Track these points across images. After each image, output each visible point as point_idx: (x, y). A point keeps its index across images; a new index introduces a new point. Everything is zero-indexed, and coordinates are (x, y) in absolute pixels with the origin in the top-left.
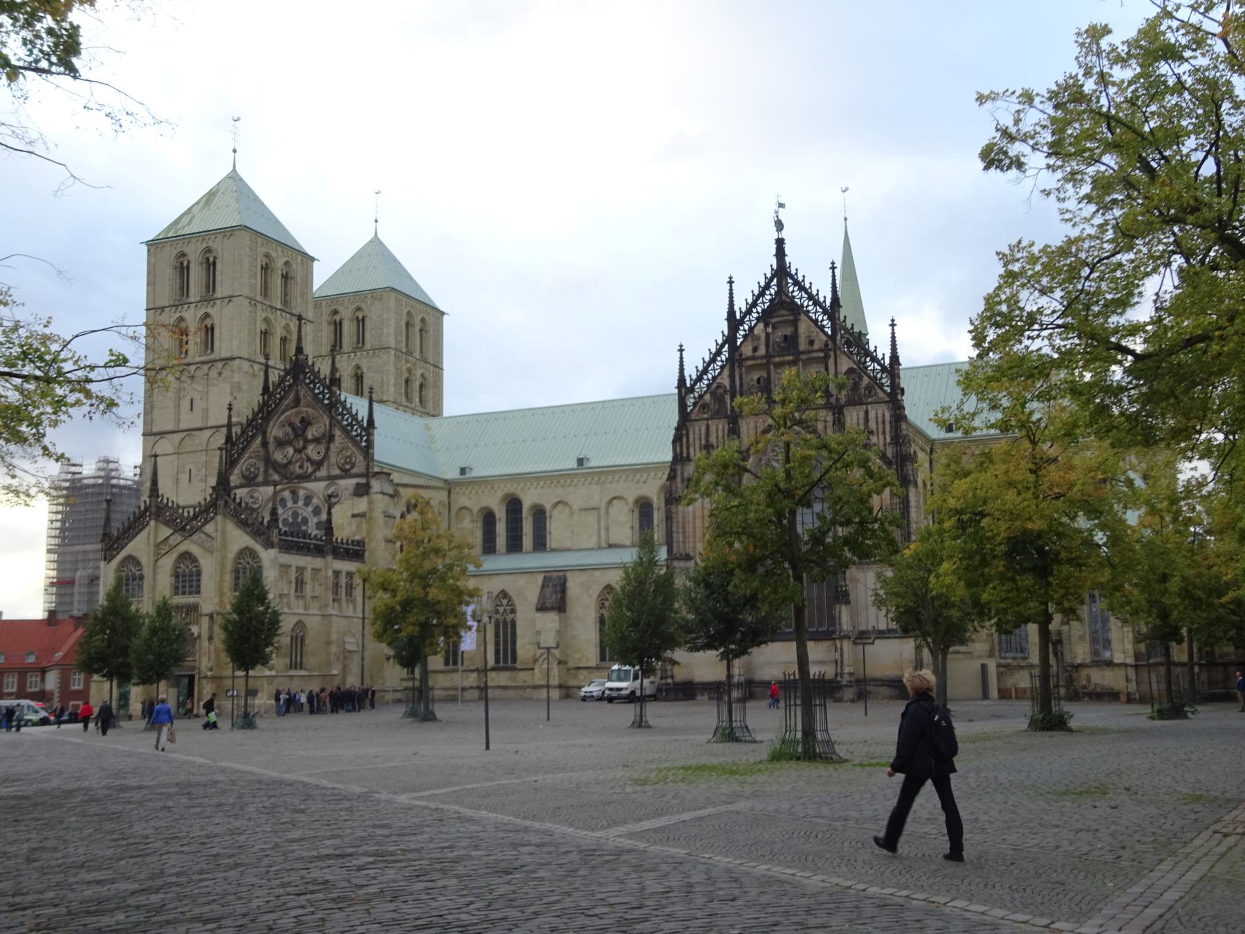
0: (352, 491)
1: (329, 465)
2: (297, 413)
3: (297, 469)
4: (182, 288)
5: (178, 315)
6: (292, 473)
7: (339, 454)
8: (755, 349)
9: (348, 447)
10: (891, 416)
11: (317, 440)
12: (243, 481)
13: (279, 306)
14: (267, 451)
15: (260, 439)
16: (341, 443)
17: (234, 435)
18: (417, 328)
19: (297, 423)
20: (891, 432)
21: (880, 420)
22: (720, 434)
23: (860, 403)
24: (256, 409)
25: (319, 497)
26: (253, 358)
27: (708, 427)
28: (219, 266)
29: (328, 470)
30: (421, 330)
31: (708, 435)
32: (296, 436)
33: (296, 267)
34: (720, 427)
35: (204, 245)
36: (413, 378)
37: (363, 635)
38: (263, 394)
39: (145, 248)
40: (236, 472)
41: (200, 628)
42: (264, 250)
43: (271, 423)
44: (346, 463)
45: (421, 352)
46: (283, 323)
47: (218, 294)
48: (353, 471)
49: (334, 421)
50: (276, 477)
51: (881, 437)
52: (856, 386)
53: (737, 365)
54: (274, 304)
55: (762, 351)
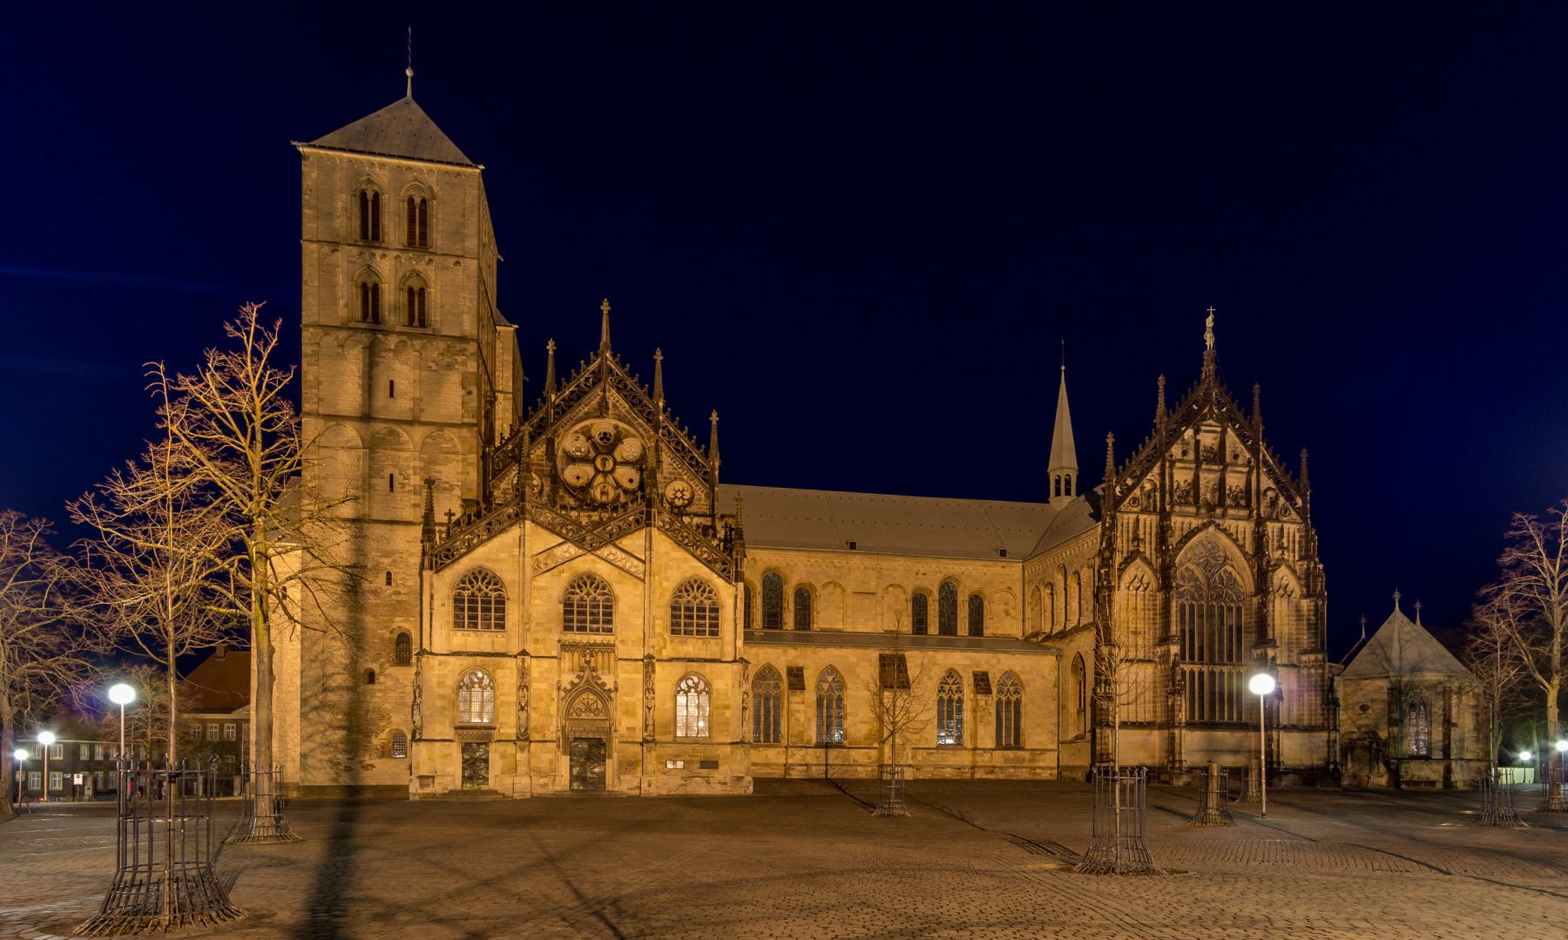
6: (594, 500)
8: (1184, 453)
10: (1300, 537)
14: (555, 467)
16: (671, 473)
19: (597, 439)
20: (1300, 551)
21: (1291, 539)
22: (1148, 530)
23: (1277, 520)
27: (1137, 520)
31: (1136, 528)
32: (598, 453)
34: (1148, 523)
49: (662, 445)
51: (1291, 554)
52: (1273, 503)
53: (1167, 464)
55: (1191, 456)
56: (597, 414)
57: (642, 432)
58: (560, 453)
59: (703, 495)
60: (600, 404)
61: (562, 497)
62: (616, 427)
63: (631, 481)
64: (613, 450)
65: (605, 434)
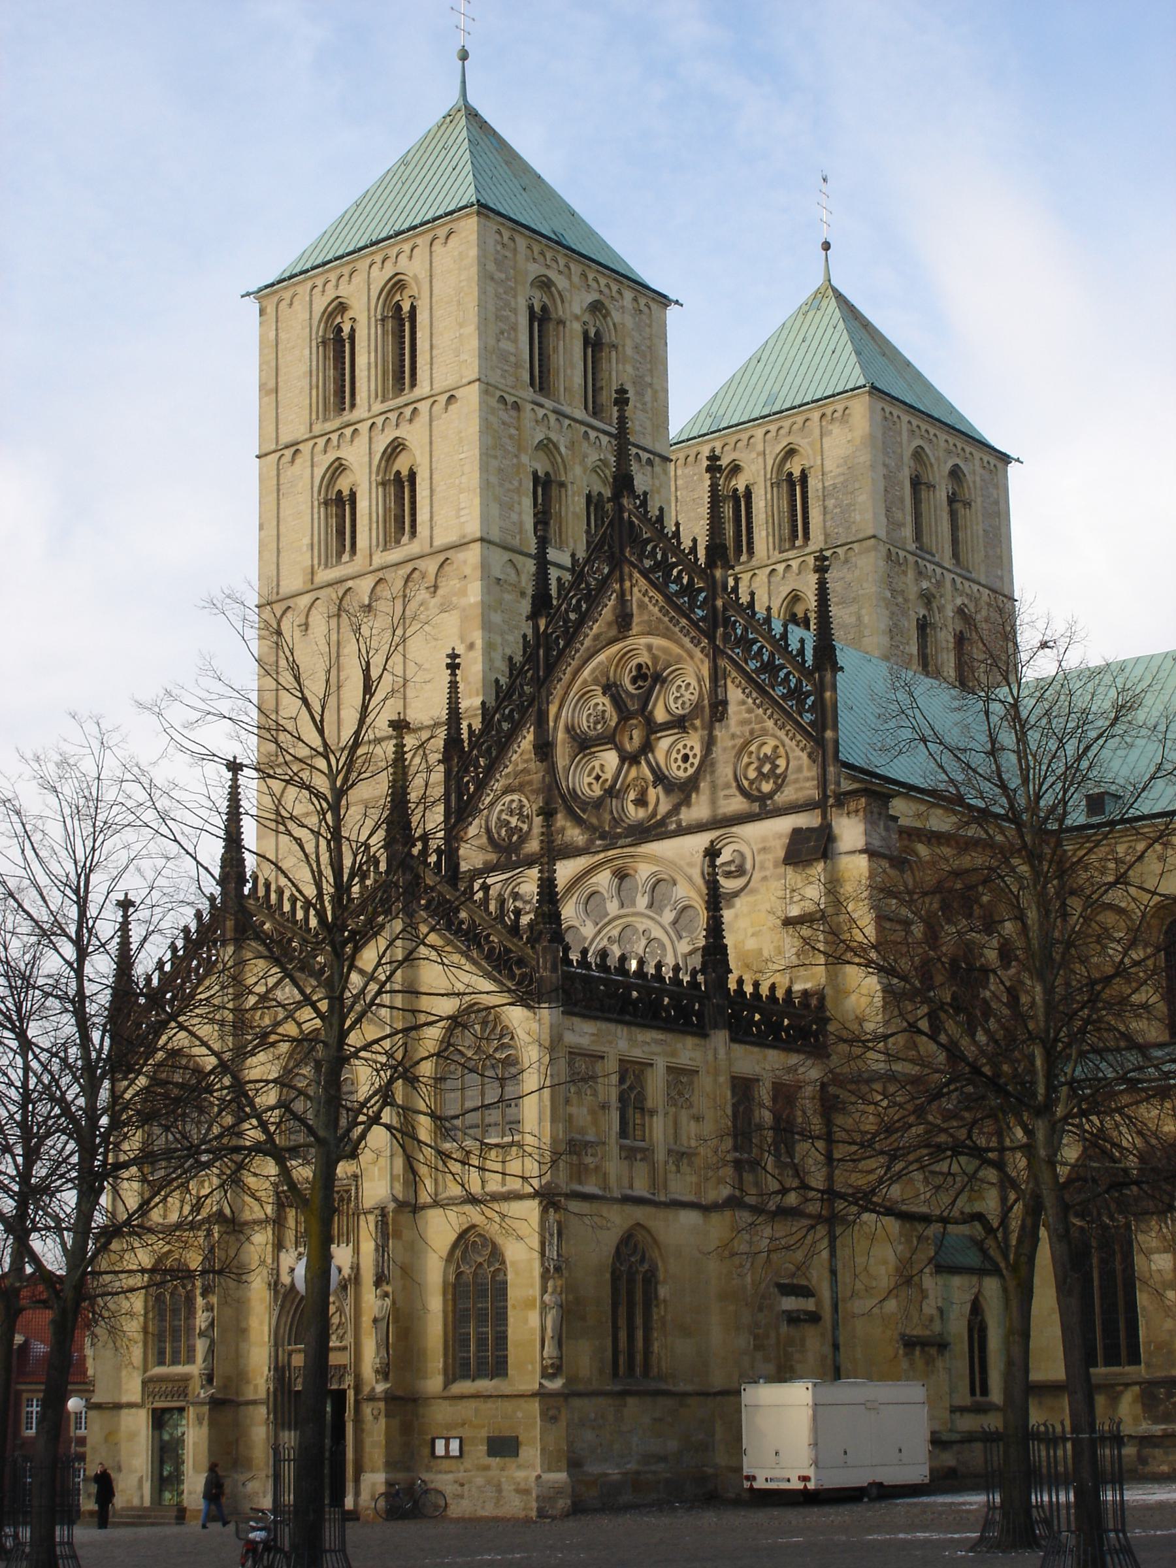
0: (781, 854)
1: (714, 787)
2: (624, 657)
3: (631, 808)
4: (340, 392)
5: (331, 456)
6: (616, 822)
7: (739, 755)
9: (765, 732)
11: (680, 724)
12: (493, 857)
13: (580, 414)
14: (552, 769)
15: (530, 737)
16: (743, 723)
17: (465, 736)
18: (942, 495)
19: (627, 682)
24: (518, 659)
25: (690, 879)
26: (516, 542)
28: (422, 318)
29: (713, 802)
30: (952, 500)
32: (625, 715)
33: (622, 314)
35: (389, 271)
36: (937, 618)
37: (833, 1272)
38: (533, 616)
39: (253, 305)
40: (472, 831)
41: (357, 1251)
42: (534, 270)
43: (559, 690)
44: (762, 776)
45: (956, 555)
46: (593, 457)
47: (423, 389)
48: (781, 798)
49: (723, 663)
50: (575, 835)
54: (567, 410)
56: (613, 632)
57: (690, 646)
58: (561, 735)
59: (804, 756)
60: (615, 608)
61: (563, 829)
62: (649, 648)
63: (686, 758)
64: (646, 704)
65: (639, 666)
